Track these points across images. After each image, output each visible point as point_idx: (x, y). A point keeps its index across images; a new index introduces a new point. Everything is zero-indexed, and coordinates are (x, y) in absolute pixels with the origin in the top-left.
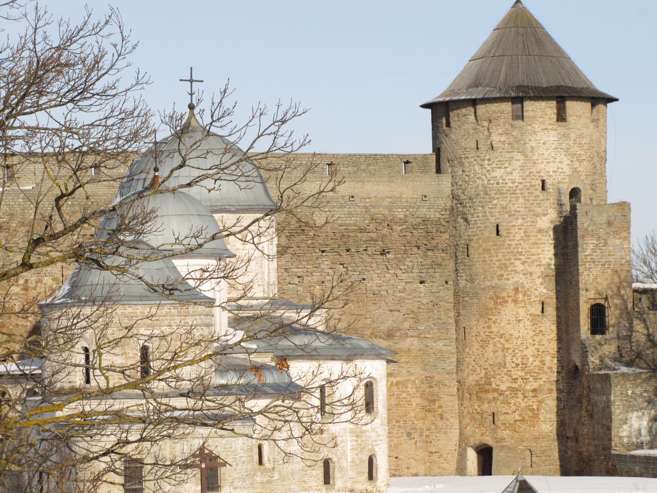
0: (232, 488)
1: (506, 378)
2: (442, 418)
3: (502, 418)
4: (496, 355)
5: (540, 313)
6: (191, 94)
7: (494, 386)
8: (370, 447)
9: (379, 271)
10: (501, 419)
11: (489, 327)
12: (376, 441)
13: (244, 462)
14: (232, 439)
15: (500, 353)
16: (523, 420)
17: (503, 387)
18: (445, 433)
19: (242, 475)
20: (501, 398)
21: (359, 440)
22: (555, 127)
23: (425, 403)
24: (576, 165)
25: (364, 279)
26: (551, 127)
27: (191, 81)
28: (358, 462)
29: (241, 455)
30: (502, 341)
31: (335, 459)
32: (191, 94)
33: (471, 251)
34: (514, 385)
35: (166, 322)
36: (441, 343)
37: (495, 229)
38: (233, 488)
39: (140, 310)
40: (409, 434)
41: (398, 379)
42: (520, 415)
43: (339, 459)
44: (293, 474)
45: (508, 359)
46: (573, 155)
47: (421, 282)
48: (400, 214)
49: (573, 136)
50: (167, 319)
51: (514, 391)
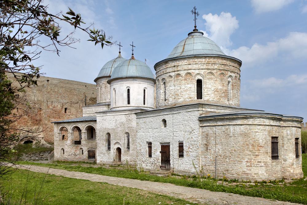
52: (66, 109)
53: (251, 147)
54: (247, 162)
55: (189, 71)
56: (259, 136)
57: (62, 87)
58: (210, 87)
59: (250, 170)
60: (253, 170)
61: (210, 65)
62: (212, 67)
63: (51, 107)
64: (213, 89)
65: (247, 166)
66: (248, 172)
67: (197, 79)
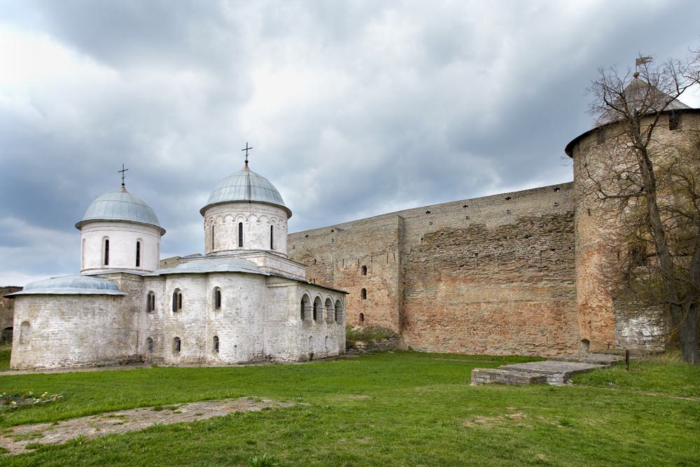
1: (596, 300)
2: (566, 324)
3: (594, 324)
15: (592, 285)
16: (607, 326)
20: (593, 312)
23: (553, 315)
31: (181, 339)
34: (600, 304)
36: (565, 284)
40: (542, 332)
41: (535, 303)
42: (604, 323)
47: (553, 250)
51: (601, 307)
52: (365, 268)
57: (358, 232)
63: (342, 270)
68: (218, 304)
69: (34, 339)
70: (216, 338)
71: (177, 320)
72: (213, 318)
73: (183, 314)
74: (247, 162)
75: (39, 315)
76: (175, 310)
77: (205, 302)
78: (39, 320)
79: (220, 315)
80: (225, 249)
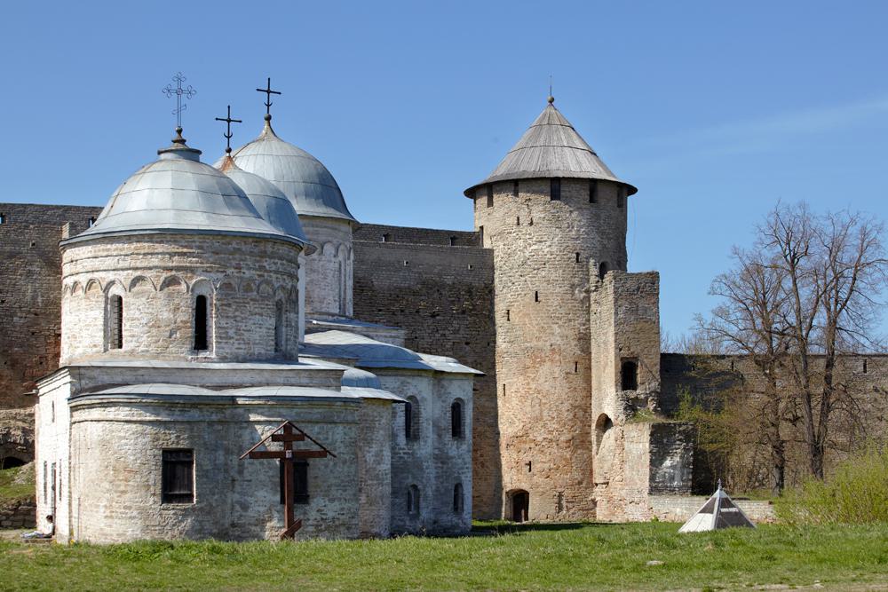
0: (327, 499)
2: (482, 467)
3: (539, 466)
4: (534, 409)
5: (574, 372)
6: (268, 105)
7: (531, 437)
8: (456, 475)
9: (430, 331)
10: (536, 467)
11: (528, 384)
12: (462, 468)
13: (345, 462)
14: (329, 426)
17: (540, 439)
18: (486, 479)
19: (343, 481)
21: (445, 466)
22: (588, 207)
24: (606, 242)
25: (416, 338)
26: (584, 206)
27: (269, 92)
28: (442, 491)
29: (341, 450)
30: (539, 396)
32: (268, 105)
33: (512, 315)
35: (234, 263)
37: (534, 296)
38: (329, 500)
39: (197, 244)
43: (425, 486)
44: (382, 497)
45: (545, 414)
46: (603, 233)
47: (467, 344)
48: (449, 280)
49: (603, 216)
50: (234, 259)
53: (112, 472)
54: (106, 506)
55: (96, 275)
56: (127, 447)
58: (137, 315)
59: (110, 526)
60: (114, 525)
61: (141, 256)
62: (145, 264)
64: (144, 321)
65: (106, 517)
66: (108, 530)
67: (110, 295)
68: (457, 431)
69: (370, 482)
70: (458, 487)
71: (413, 454)
72: (453, 451)
73: (422, 443)
74: (268, 119)
75: (374, 437)
76: (408, 435)
77: (436, 425)
78: (375, 448)
79: (464, 447)
80: (323, 310)
